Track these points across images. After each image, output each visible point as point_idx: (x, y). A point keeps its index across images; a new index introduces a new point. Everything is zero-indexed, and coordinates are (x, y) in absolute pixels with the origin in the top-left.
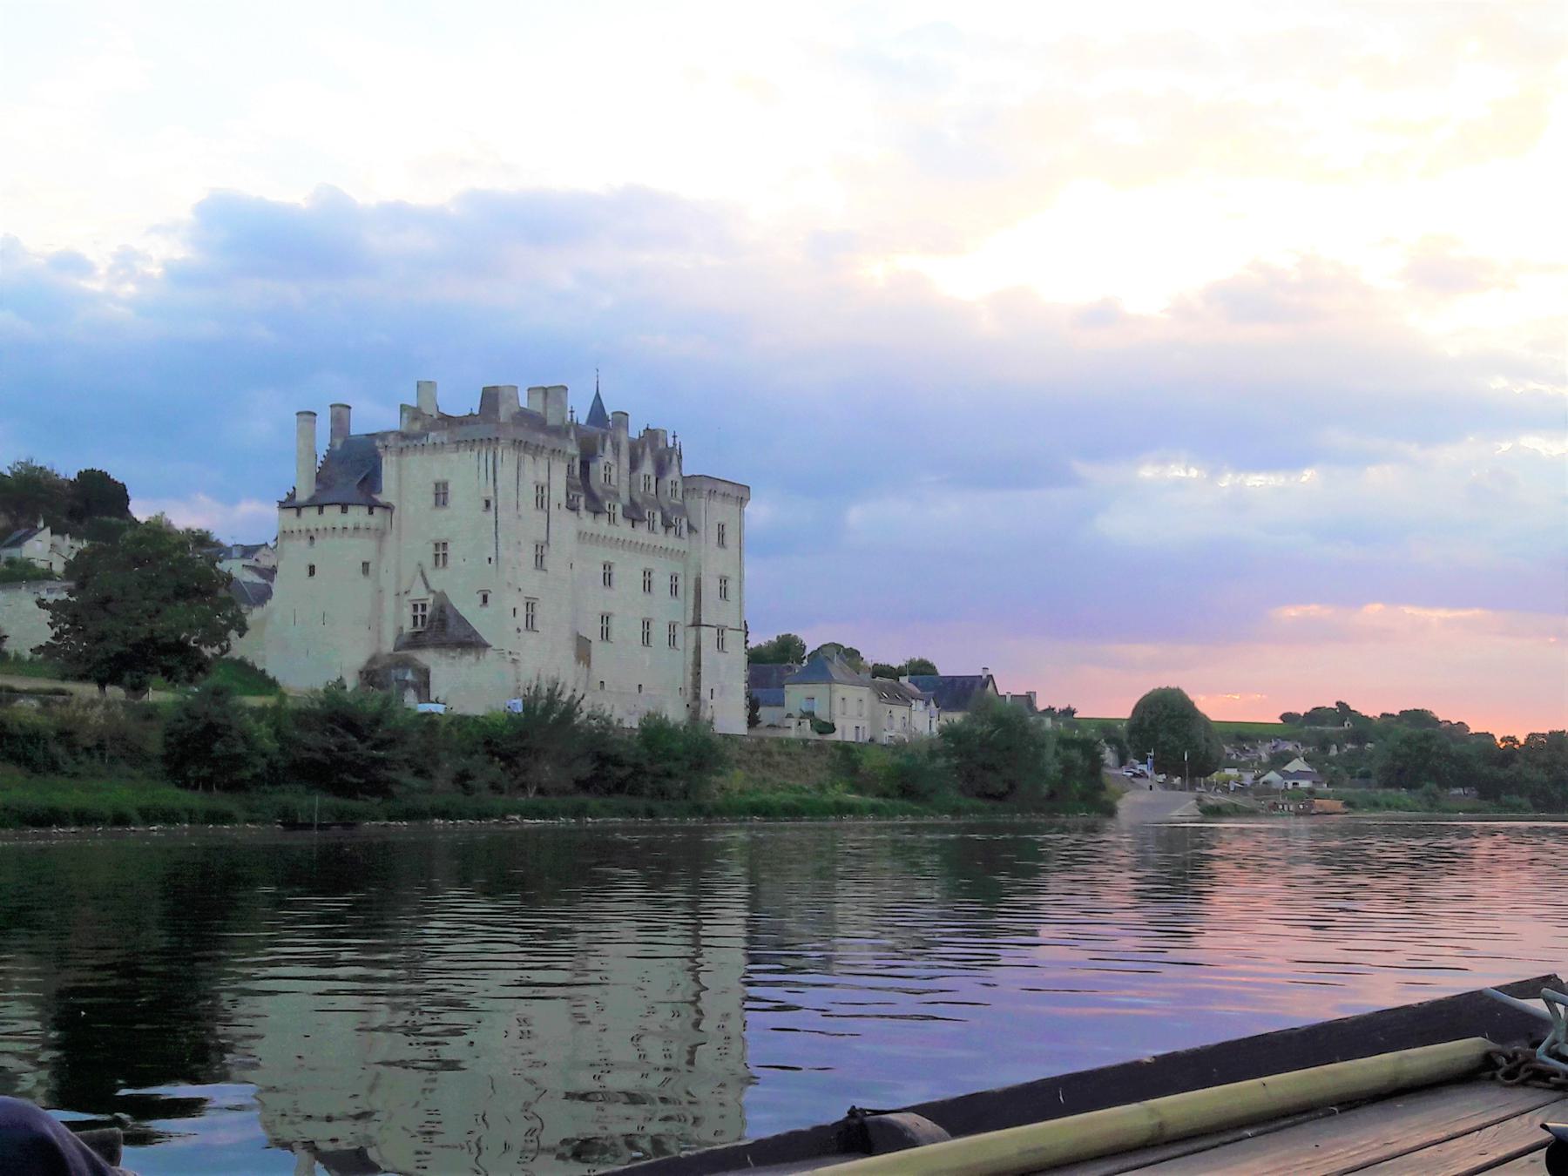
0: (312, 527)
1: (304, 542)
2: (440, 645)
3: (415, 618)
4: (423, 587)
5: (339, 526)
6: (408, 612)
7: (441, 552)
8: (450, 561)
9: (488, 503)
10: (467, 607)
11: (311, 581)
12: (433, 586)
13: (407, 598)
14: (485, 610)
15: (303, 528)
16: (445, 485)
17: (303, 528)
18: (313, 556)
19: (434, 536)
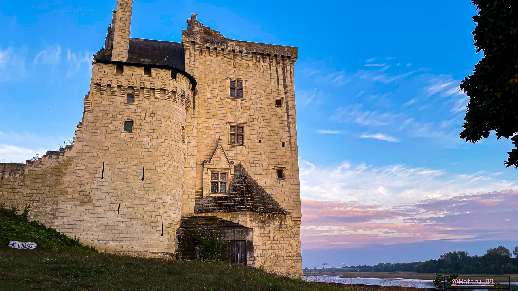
0: (137, 85)
1: (121, 99)
2: (252, 210)
3: (214, 184)
4: (225, 159)
5: (170, 88)
6: (208, 178)
7: (237, 134)
8: (247, 141)
9: (279, 103)
10: (265, 181)
11: (128, 136)
12: (230, 159)
13: (206, 166)
14: (281, 182)
15: (125, 84)
16: (241, 82)
17: (125, 84)
18: (133, 111)
19: (231, 119)
